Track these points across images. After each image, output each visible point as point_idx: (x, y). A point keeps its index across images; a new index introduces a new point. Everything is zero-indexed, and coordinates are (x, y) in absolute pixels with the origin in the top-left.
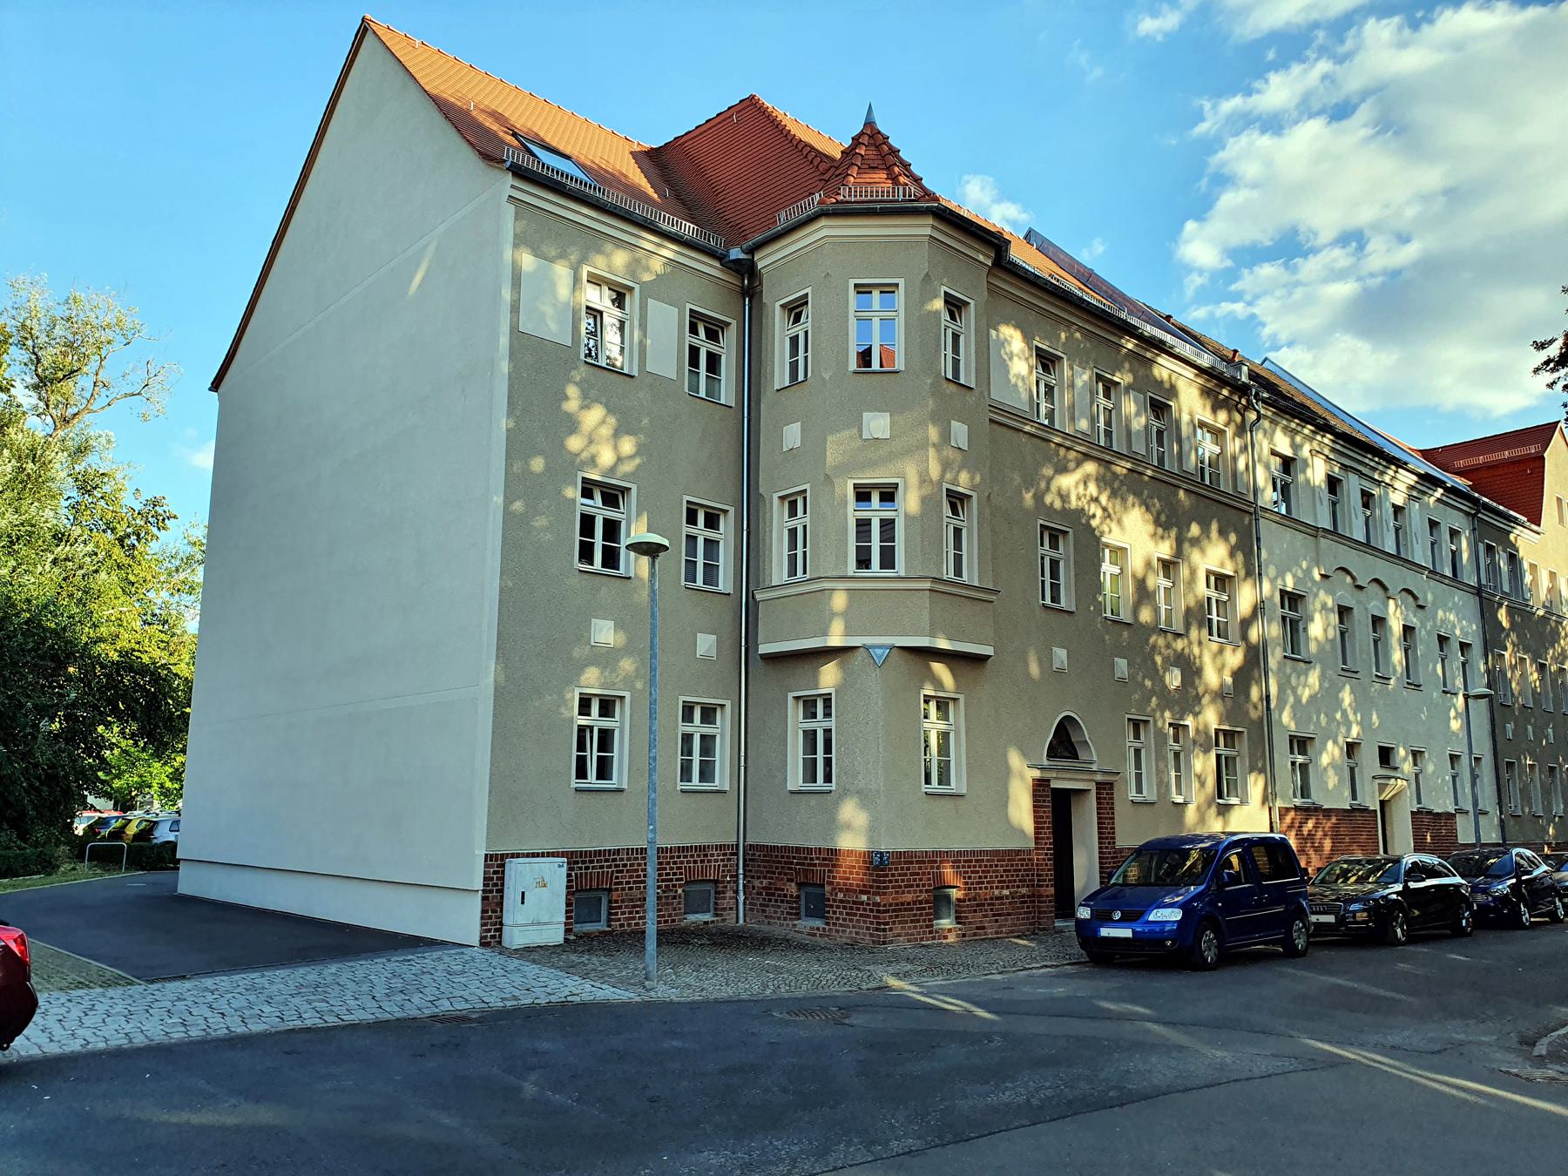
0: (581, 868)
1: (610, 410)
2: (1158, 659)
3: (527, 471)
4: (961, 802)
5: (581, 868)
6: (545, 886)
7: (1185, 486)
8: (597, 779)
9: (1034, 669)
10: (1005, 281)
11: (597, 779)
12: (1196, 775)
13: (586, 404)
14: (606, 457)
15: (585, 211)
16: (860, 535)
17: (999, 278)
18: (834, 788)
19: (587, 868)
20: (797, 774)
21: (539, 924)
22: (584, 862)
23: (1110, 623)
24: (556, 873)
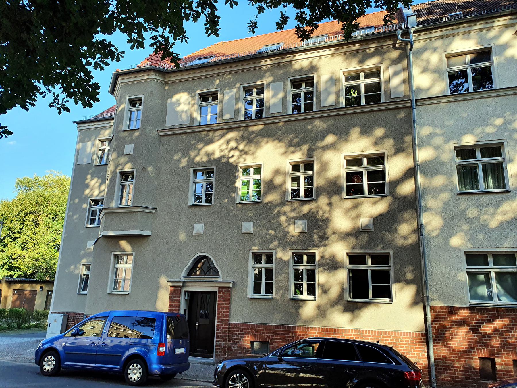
0: (76, 318)
1: (99, 178)
2: (283, 218)
3: (74, 203)
4: (127, 297)
5: (76, 318)
6: (56, 322)
7: (282, 120)
8: (266, 293)
9: (182, 237)
10: (173, 77)
11: (266, 293)
12: (319, 284)
13: (92, 179)
14: (96, 192)
15: (87, 125)
16: (496, 164)
17: (171, 77)
18: (274, 297)
19: (78, 318)
20: (468, 293)
21: (53, 333)
22: (77, 316)
23: (240, 206)
24: (60, 318)
